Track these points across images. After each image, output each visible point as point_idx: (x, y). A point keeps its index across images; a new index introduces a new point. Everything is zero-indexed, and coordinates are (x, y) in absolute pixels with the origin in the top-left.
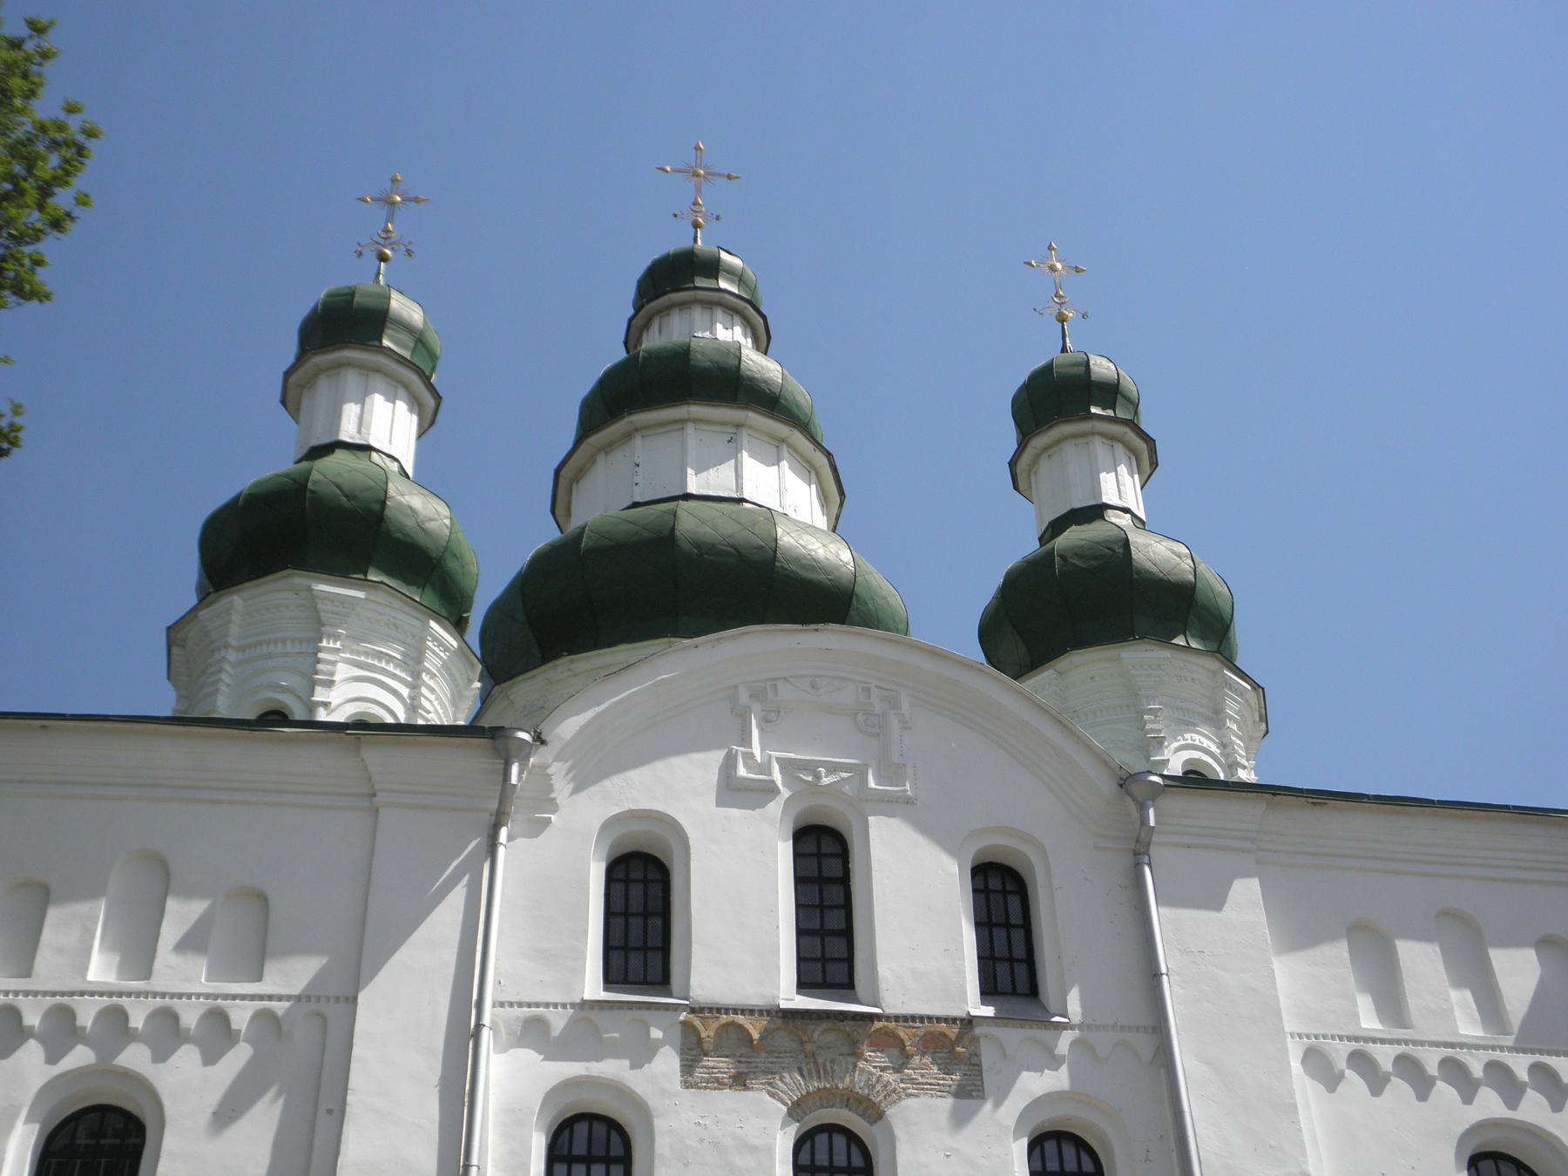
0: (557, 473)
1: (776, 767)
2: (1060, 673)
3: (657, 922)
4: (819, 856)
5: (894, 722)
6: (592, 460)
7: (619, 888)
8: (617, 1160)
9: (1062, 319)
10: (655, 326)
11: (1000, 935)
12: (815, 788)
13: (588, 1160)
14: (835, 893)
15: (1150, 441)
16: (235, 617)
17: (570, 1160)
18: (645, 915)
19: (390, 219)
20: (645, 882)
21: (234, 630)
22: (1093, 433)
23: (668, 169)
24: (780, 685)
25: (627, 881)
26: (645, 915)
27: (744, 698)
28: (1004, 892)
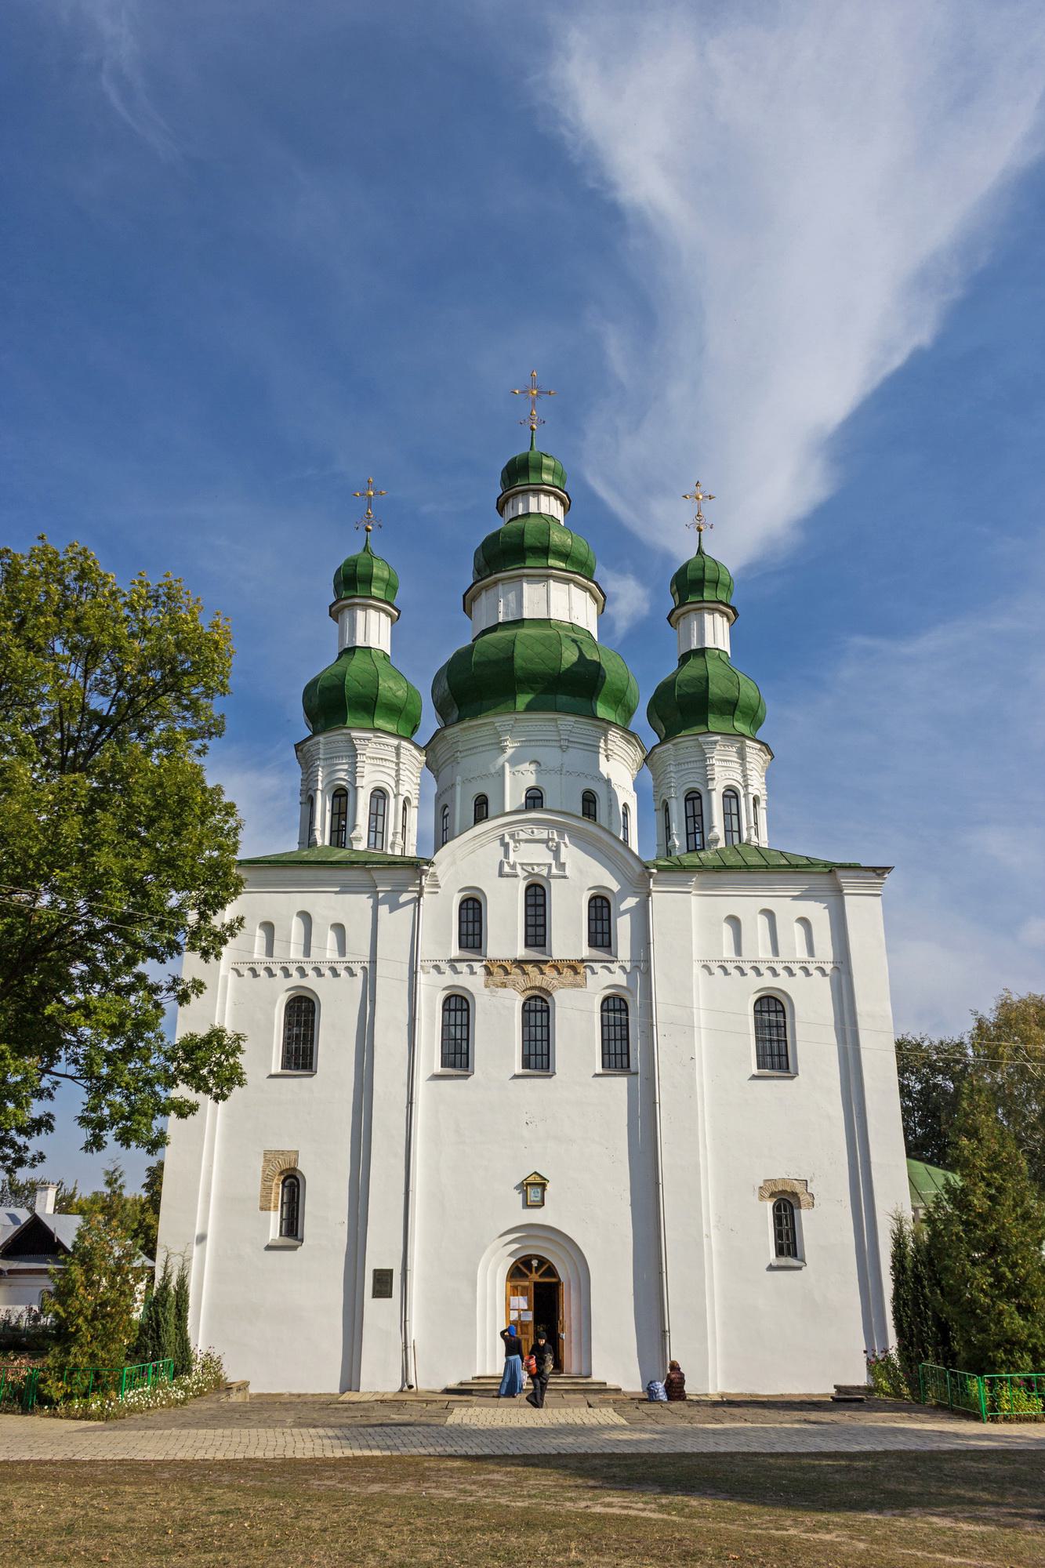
0: (464, 596)
1: (519, 867)
2: (674, 745)
3: (477, 925)
4: (536, 895)
5: (562, 846)
6: (479, 593)
7: (464, 912)
8: (465, 1010)
9: (700, 530)
10: (510, 504)
11: (599, 922)
12: (531, 875)
13: (456, 1010)
14: (540, 911)
15: (733, 609)
16: (321, 746)
17: (450, 1010)
18: (474, 922)
19: (369, 506)
20: (474, 909)
21: (321, 751)
22: (704, 608)
23: (517, 392)
24: (521, 832)
25: (467, 909)
26: (474, 922)
27: (507, 839)
28: (602, 907)
